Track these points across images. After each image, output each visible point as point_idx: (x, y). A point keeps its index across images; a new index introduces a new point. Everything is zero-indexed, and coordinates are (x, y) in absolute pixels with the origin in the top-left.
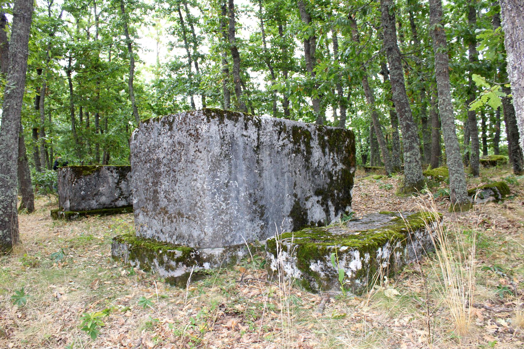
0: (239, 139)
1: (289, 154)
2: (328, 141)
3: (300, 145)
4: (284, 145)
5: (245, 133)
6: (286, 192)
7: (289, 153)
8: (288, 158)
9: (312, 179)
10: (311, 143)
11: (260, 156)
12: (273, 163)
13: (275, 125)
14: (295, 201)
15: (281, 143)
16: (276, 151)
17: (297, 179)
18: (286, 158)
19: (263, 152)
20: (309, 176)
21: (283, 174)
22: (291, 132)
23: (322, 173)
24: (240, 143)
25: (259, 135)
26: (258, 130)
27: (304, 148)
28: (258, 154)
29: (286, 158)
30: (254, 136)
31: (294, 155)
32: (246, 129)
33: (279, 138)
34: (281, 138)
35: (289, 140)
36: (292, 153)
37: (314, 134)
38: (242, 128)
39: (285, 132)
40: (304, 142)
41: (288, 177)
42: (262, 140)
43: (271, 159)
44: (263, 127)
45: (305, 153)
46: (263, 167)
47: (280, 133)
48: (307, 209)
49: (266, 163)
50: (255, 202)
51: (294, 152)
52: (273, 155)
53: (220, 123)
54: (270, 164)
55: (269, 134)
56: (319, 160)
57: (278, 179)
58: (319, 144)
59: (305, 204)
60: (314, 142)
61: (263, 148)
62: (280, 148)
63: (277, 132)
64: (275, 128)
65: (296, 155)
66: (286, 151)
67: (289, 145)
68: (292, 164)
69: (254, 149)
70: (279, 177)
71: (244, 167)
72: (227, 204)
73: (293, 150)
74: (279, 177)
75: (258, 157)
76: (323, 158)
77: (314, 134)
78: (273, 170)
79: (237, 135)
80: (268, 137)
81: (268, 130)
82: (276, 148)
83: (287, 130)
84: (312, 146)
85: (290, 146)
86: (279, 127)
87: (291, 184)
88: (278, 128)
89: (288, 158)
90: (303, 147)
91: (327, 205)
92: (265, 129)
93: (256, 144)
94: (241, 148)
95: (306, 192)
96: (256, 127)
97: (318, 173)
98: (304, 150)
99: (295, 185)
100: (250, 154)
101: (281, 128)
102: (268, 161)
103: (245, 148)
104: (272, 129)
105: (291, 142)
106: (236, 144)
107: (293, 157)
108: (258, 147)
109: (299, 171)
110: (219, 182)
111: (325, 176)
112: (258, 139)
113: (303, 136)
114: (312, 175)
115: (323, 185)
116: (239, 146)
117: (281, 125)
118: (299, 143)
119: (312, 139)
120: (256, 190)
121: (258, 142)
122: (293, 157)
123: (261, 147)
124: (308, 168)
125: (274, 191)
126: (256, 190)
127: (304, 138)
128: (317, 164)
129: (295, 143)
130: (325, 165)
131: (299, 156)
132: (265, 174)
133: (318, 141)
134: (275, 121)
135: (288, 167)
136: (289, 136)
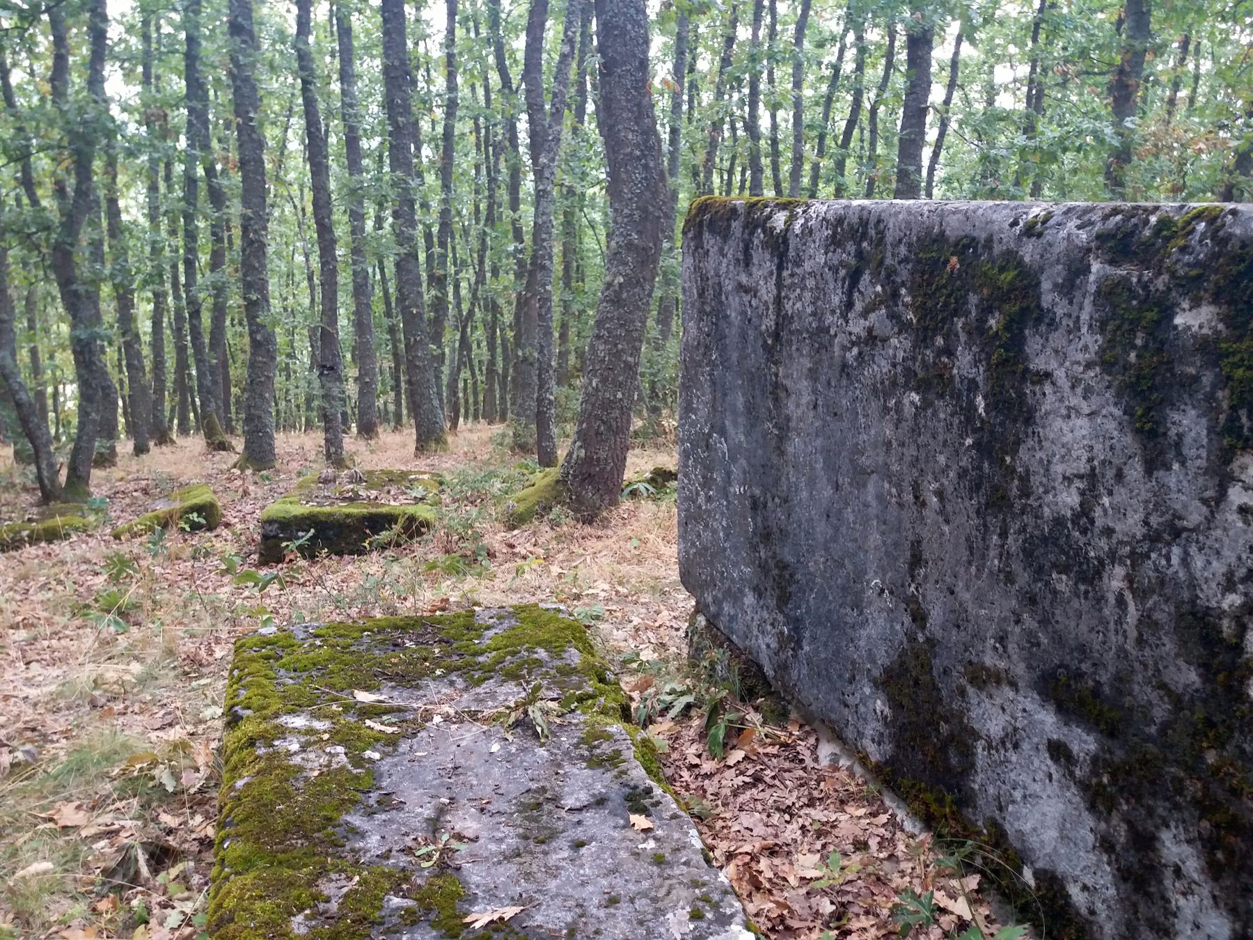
0: (730, 298)
1: (886, 389)
2: (1207, 348)
3: (949, 352)
4: (872, 339)
5: (744, 279)
6: (872, 568)
7: (894, 384)
8: (886, 410)
9: (1023, 578)
10: (1033, 344)
11: (781, 371)
12: (820, 409)
13: (834, 242)
14: (912, 638)
15: (857, 327)
16: (837, 360)
17: (925, 534)
18: (875, 406)
19: (790, 357)
20: (1005, 555)
21: (860, 475)
22: (904, 273)
23: (1115, 580)
24: (733, 315)
25: (779, 285)
26: (780, 268)
27: (980, 374)
28: (776, 363)
29: (875, 406)
30: (767, 292)
31: (915, 397)
32: (748, 262)
33: (849, 305)
34: (859, 306)
35: (894, 316)
36: (907, 387)
37: (1068, 288)
38: (738, 260)
39: (875, 275)
40: (978, 330)
41: (880, 498)
42: (788, 306)
43: (815, 391)
44: (792, 253)
45: (980, 402)
46: (788, 419)
47: (855, 277)
48: (976, 735)
49: (798, 406)
50: (766, 536)
51: (911, 380)
52: (823, 378)
53: (697, 248)
54: (811, 414)
55: (810, 283)
56: (1092, 477)
57: (837, 487)
58: (1106, 362)
59: (962, 693)
60: (1057, 339)
61: (790, 342)
62: (855, 351)
63: (843, 272)
64: (837, 257)
65: (926, 404)
66: (880, 367)
67: (894, 341)
68: (902, 445)
69: (765, 342)
70: (845, 481)
71: (740, 402)
72: (709, 499)
73: (909, 373)
74: (845, 481)
75: (776, 375)
76: (1135, 471)
77: (1068, 288)
78: (819, 442)
79: (729, 286)
80: (808, 295)
81: (808, 265)
82: (837, 350)
83: (889, 261)
84: (1039, 363)
85: (899, 345)
86: (851, 247)
87: (896, 544)
88: (847, 255)
89: (886, 410)
90: (964, 363)
91: (1145, 842)
92: (798, 263)
93: (769, 323)
94: (734, 331)
95: (978, 636)
96: (772, 255)
97: (1090, 575)
98: (973, 385)
99: (916, 560)
100: (756, 358)
101: (860, 254)
102: (806, 399)
103: (743, 336)
104: (821, 259)
105: (903, 327)
106: (726, 317)
107: (908, 411)
108: (777, 336)
109: (940, 494)
110: (693, 424)
111: (1147, 620)
112: (778, 301)
113: (973, 299)
114: (1028, 553)
115: (1120, 679)
116: (730, 324)
117: (864, 236)
118: (950, 335)
119: (1043, 319)
120: (769, 495)
121: (778, 315)
122: (908, 411)
123: (784, 334)
124: (997, 503)
125: (822, 529)
126: (769, 495)
127: (986, 310)
128: (1069, 499)
129: (923, 337)
130: (1153, 538)
131: (944, 409)
132: (795, 445)
133: (1092, 341)
134: (840, 220)
135: (882, 451)
136: (895, 295)
